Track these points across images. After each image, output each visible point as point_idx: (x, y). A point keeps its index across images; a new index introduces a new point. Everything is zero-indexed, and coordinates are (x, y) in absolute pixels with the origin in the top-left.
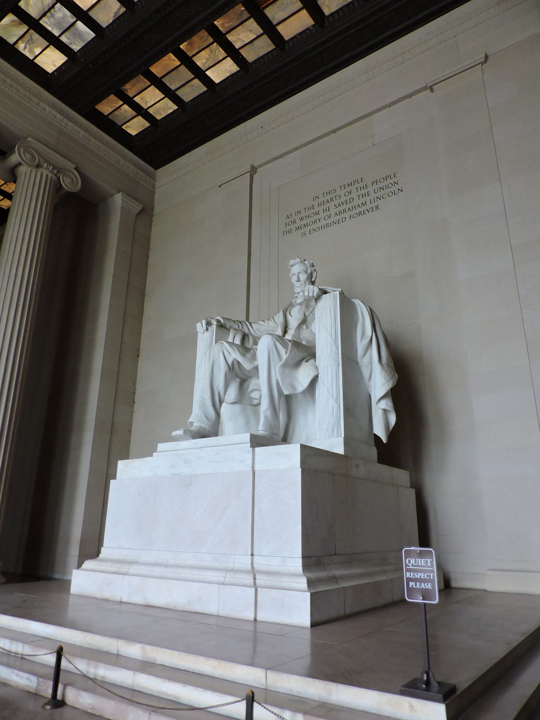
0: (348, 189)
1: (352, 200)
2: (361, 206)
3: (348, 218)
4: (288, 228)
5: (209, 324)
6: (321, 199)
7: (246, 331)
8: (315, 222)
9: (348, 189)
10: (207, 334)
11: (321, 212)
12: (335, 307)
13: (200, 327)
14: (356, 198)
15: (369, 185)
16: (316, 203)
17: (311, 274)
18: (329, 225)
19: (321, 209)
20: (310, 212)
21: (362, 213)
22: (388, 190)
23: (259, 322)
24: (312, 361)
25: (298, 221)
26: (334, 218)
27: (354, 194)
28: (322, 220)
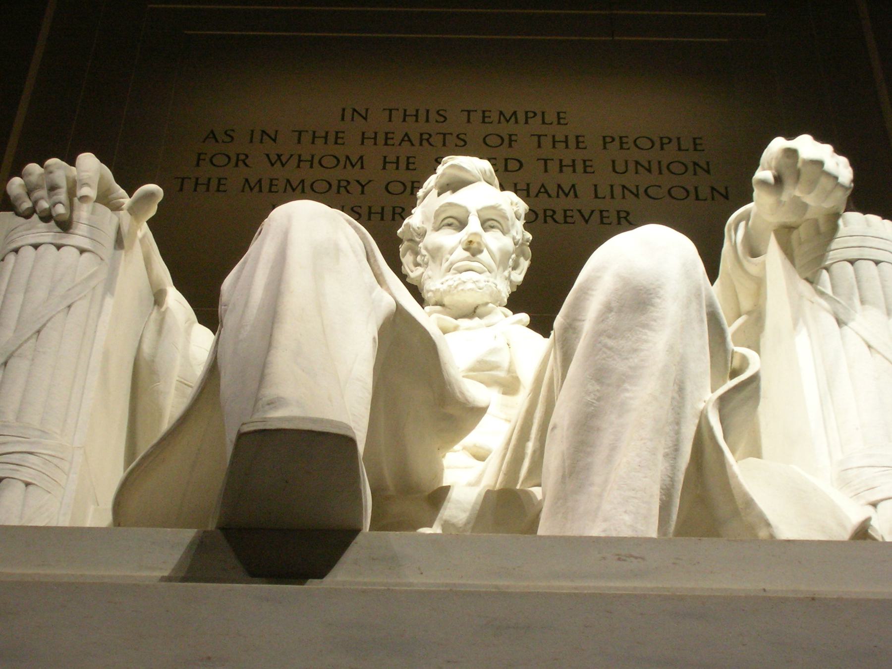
0: (505, 129)
9: (505, 129)
21: (559, 217)
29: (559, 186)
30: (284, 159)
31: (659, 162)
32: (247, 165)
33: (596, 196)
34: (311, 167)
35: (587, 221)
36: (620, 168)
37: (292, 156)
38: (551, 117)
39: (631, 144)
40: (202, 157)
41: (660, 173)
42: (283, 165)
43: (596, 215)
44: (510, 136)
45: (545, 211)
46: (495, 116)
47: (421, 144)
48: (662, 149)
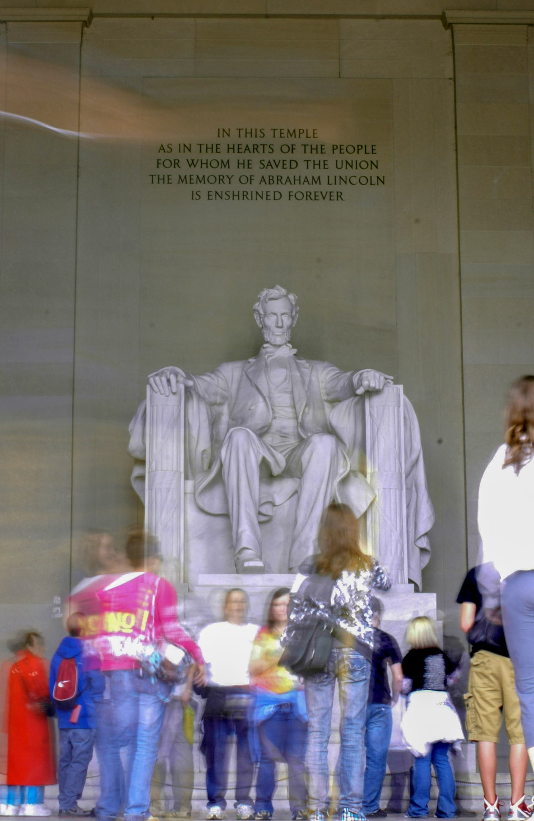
1: (294, 164)
2: (310, 183)
3: (285, 195)
4: (162, 171)
6: (234, 139)
8: (221, 179)
9: (291, 141)
10: (173, 399)
14: (302, 165)
15: (328, 149)
18: (249, 196)
19: (233, 157)
20: (210, 156)
21: (313, 196)
22: (359, 172)
23: (205, 378)
25: (183, 163)
27: (299, 155)
28: (235, 180)
29: (313, 178)
30: (195, 162)
31: (356, 161)
32: (179, 167)
33: (329, 184)
34: (207, 167)
35: (324, 198)
36: (339, 166)
37: (198, 160)
38: (310, 134)
39: (345, 151)
40: (160, 162)
41: (356, 168)
42: (195, 166)
43: (328, 194)
44: (292, 145)
45: (307, 192)
46: (285, 132)
47: (254, 152)
48: (358, 153)
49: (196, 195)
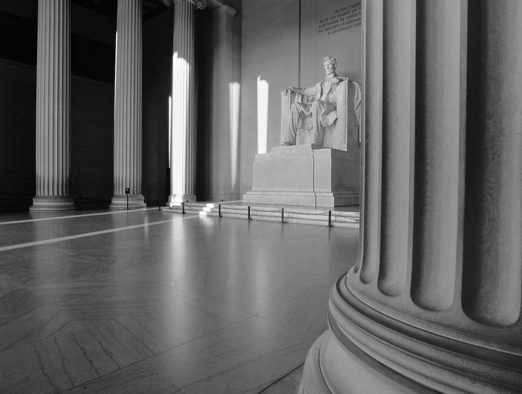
0: (354, 8)
3: (353, 26)
5: (287, 92)
7: (303, 93)
8: (336, 26)
9: (354, 8)
11: (339, 21)
12: (346, 88)
13: (283, 93)
16: (336, 15)
17: (334, 64)
19: (339, 18)
24: (335, 112)
25: (326, 25)
26: (346, 26)
28: (340, 25)
49: (329, 33)
